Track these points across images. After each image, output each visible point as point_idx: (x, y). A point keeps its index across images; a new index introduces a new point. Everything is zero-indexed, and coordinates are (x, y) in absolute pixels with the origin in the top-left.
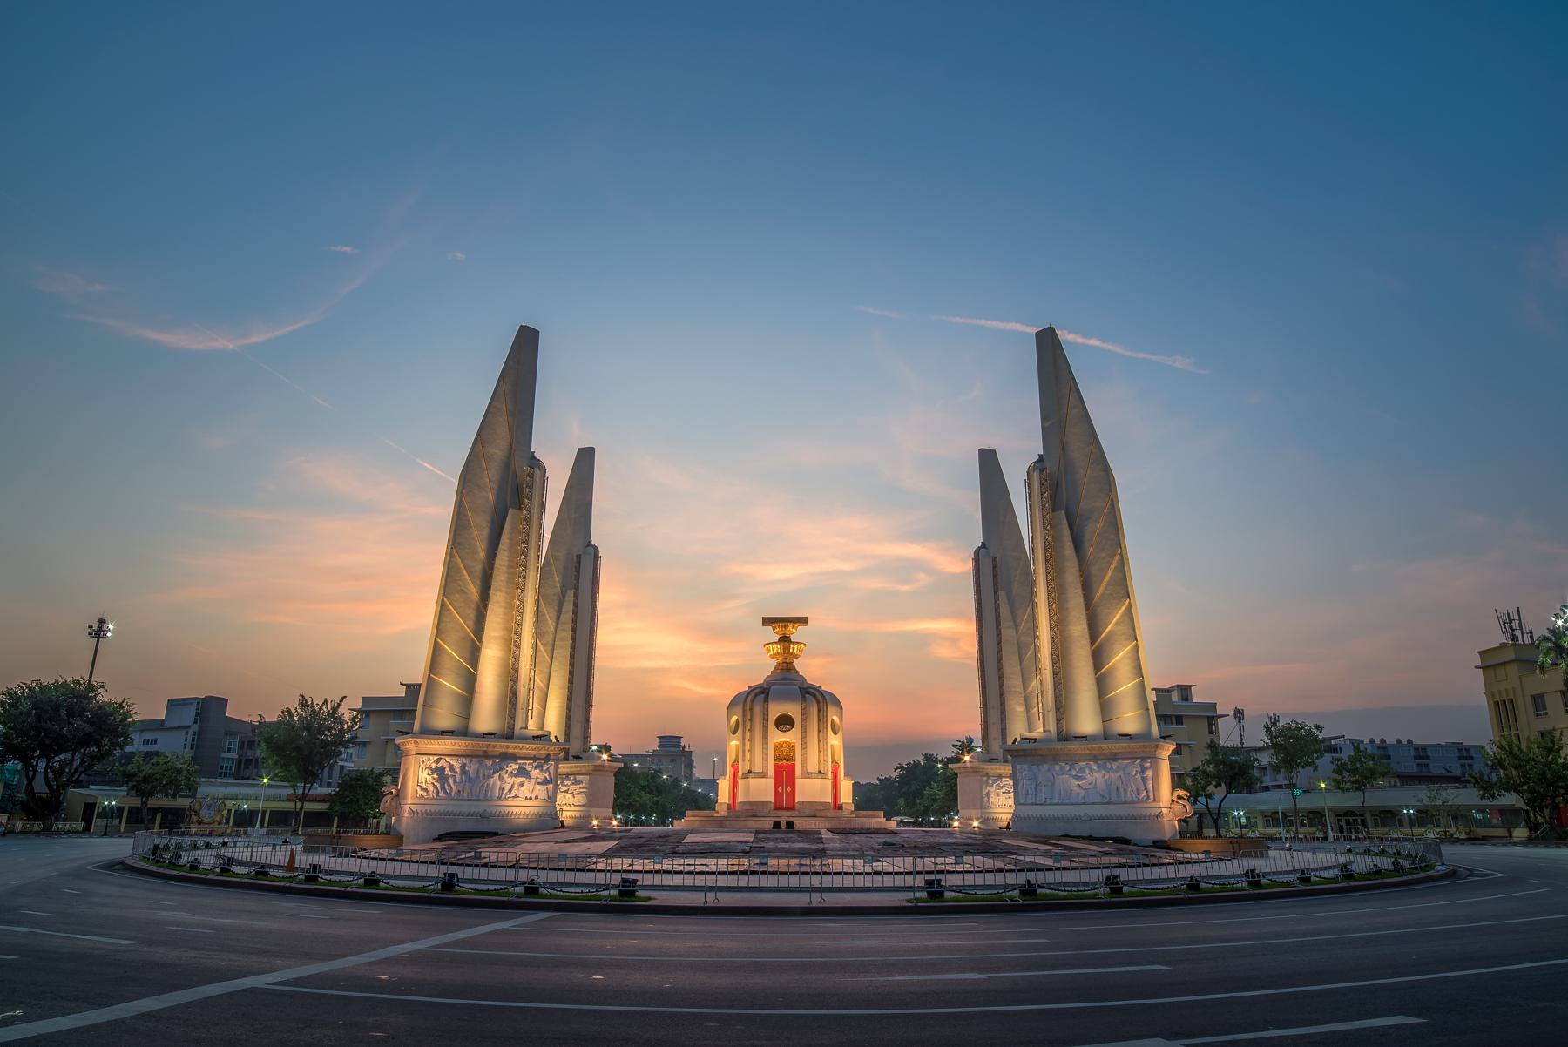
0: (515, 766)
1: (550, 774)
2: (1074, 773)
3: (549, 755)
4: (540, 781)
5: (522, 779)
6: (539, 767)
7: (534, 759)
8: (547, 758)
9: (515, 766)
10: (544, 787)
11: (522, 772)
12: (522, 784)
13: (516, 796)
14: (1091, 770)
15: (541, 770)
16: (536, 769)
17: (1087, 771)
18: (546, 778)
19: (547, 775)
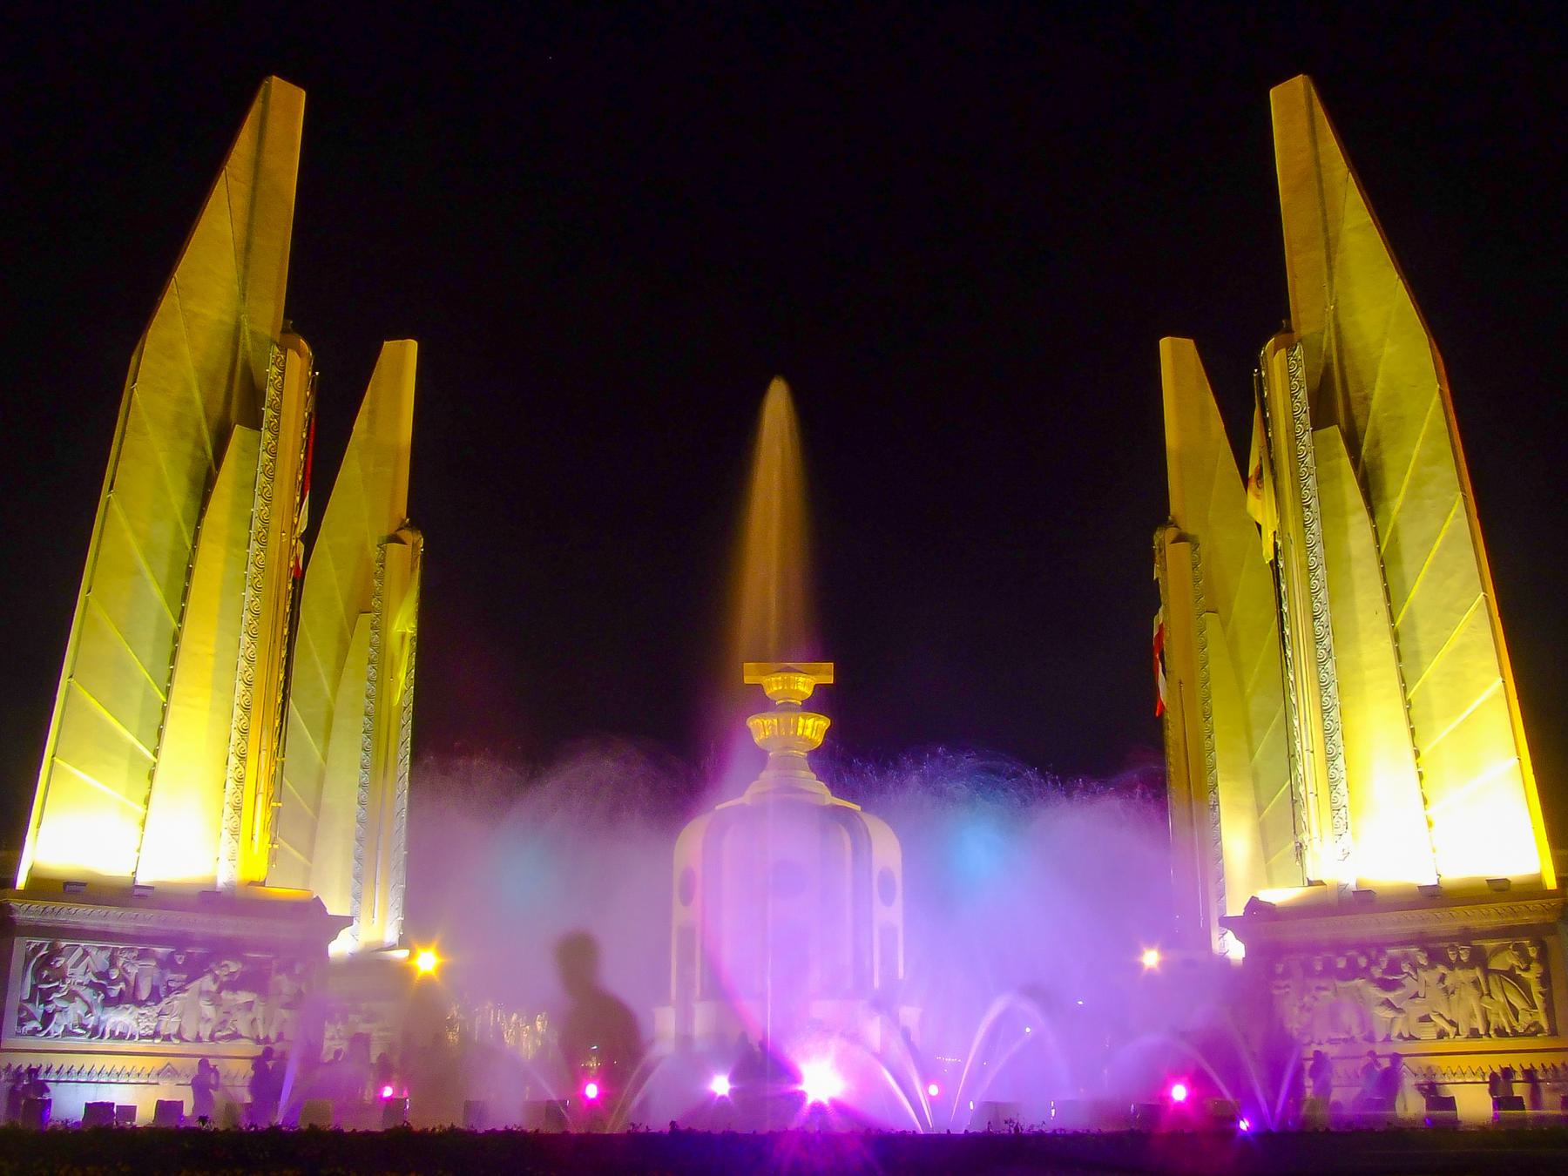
2: (1377, 972)
9: (234, 967)
14: (1415, 967)
17: (1406, 968)
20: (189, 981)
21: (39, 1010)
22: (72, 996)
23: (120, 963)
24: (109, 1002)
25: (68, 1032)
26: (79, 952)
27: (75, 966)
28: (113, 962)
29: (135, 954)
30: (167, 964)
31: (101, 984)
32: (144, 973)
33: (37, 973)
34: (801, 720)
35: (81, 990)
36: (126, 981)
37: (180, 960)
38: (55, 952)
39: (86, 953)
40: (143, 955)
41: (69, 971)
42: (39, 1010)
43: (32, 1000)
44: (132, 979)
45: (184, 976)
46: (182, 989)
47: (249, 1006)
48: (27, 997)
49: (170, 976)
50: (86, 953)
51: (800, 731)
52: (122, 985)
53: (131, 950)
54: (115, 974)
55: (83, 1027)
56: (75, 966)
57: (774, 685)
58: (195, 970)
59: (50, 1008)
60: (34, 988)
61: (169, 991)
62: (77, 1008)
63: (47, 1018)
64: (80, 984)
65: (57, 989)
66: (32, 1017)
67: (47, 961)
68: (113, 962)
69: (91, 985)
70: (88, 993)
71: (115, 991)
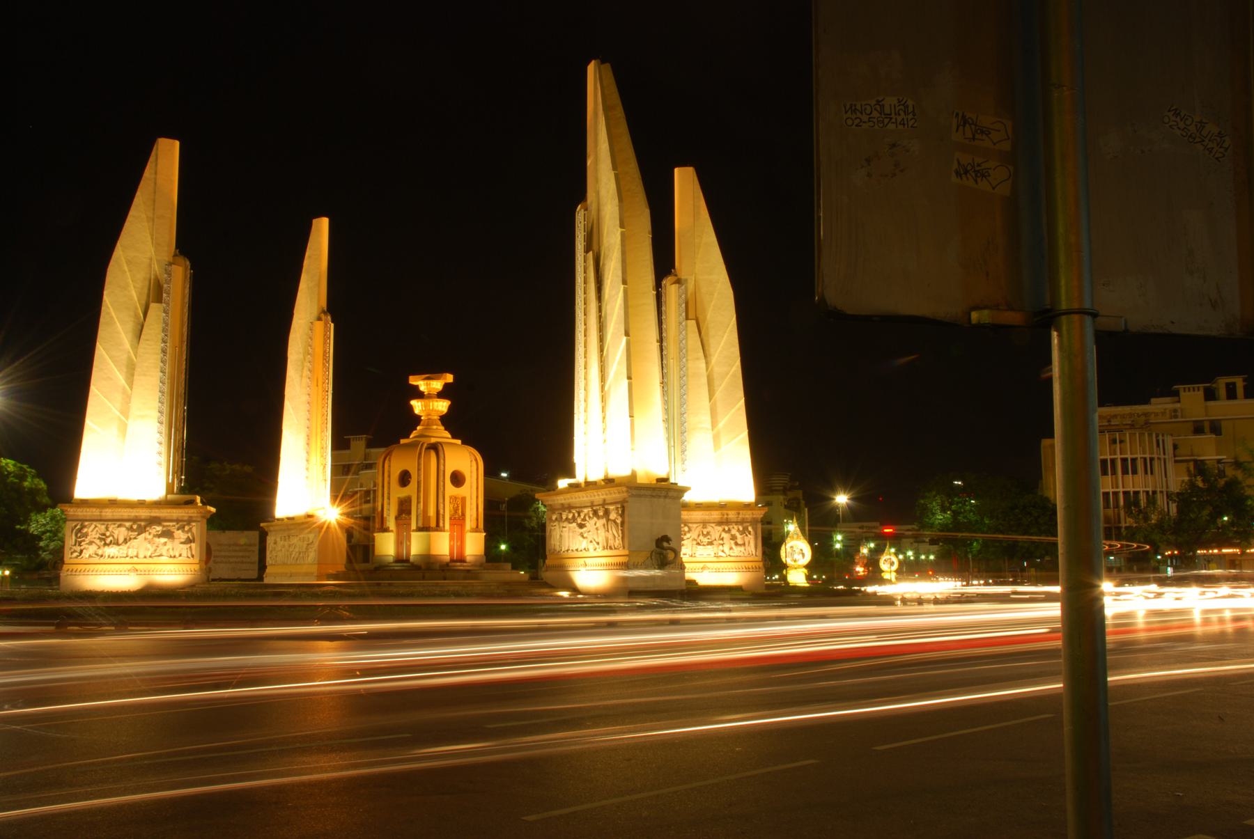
3: (191, 517)
4: (183, 540)
5: (165, 540)
7: (178, 521)
9: (159, 528)
10: (189, 546)
11: (168, 534)
15: (183, 531)
16: (178, 529)
18: (188, 537)
19: (189, 535)
20: (138, 535)
22: (91, 543)
23: (110, 529)
24: (105, 544)
26: (93, 526)
27: (92, 531)
28: (107, 529)
29: (116, 525)
30: (131, 529)
31: (103, 538)
32: (121, 533)
34: (431, 404)
35: (95, 540)
36: (113, 536)
37: (135, 527)
38: (83, 527)
39: (96, 526)
40: (119, 526)
41: (90, 533)
42: (78, 549)
43: (75, 545)
44: (116, 537)
45: (136, 533)
46: (135, 538)
47: (165, 544)
48: (73, 544)
49: (130, 533)
50: (96, 526)
51: (431, 408)
52: (111, 538)
53: (114, 524)
54: (108, 534)
55: (97, 555)
56: (92, 531)
57: (422, 385)
58: (141, 530)
59: (82, 548)
60: (76, 541)
61: (130, 539)
62: (92, 549)
64: (95, 538)
65: (84, 541)
67: (80, 530)
68: (107, 529)
69: (99, 538)
70: (98, 541)
71: (108, 541)
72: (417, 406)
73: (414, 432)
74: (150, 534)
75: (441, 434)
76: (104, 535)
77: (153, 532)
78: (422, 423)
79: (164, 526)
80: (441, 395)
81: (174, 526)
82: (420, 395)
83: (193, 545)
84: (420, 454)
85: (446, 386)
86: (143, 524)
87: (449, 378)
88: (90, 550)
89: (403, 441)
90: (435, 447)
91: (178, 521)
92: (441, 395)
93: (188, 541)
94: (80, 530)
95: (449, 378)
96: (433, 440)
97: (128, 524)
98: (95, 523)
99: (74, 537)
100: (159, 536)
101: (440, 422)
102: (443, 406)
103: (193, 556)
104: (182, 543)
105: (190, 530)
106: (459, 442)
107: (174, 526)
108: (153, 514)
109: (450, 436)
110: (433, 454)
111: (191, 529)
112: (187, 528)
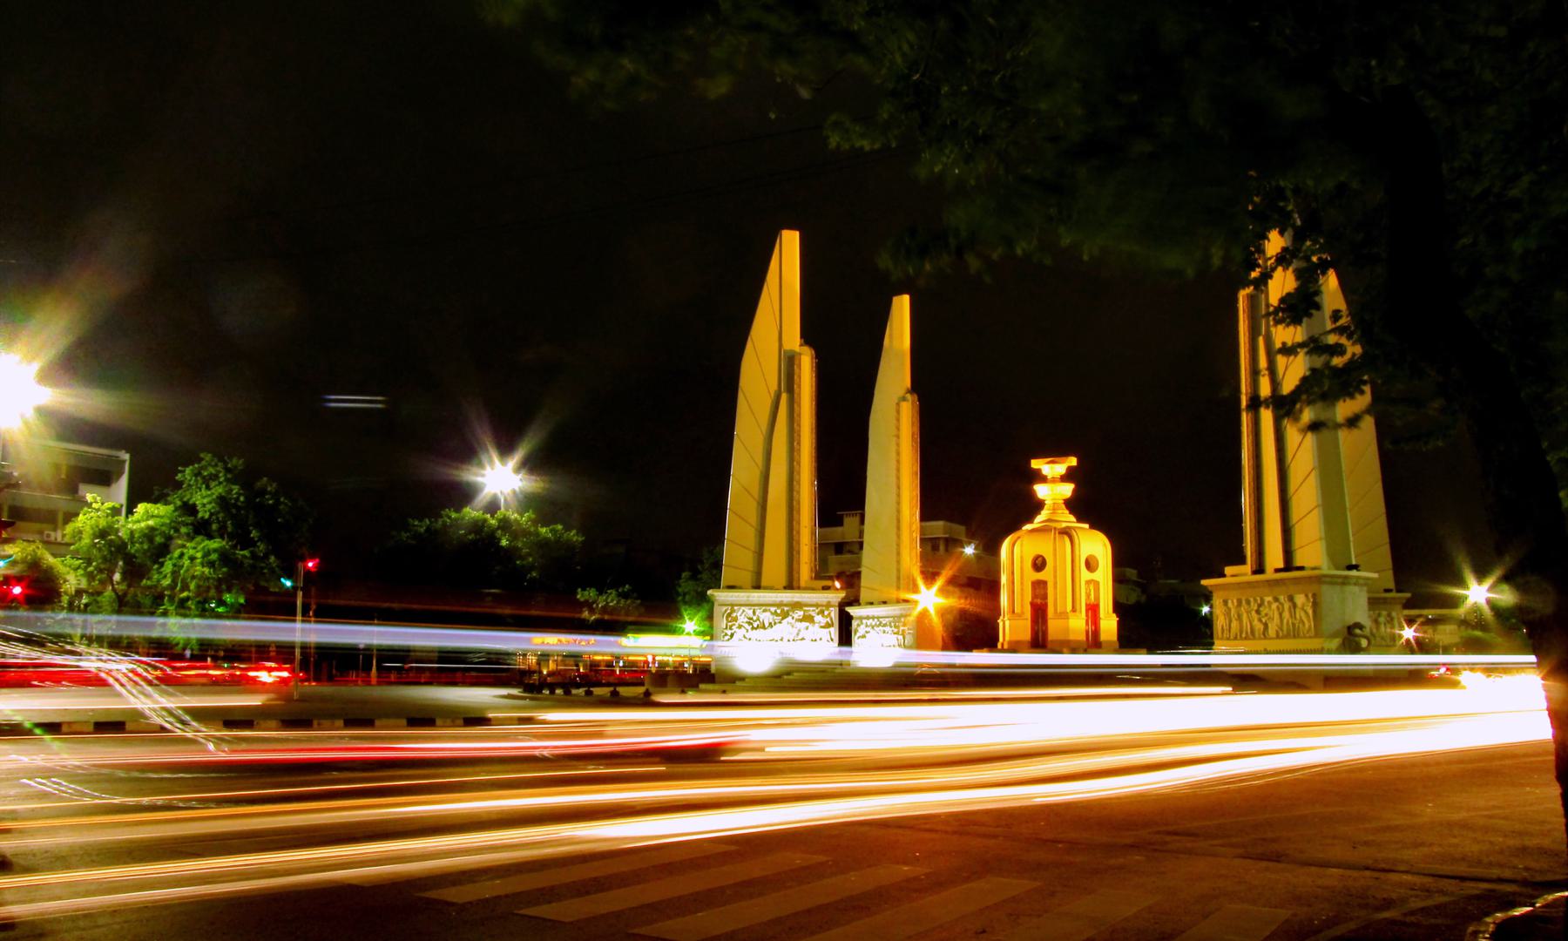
0: (801, 613)
1: (831, 619)
4: (823, 625)
5: (808, 624)
6: (822, 612)
8: (829, 605)
9: (801, 613)
10: (828, 630)
11: (808, 619)
12: (807, 628)
13: (803, 639)
16: (818, 614)
19: (828, 619)
20: (783, 619)
21: (729, 632)
22: (740, 627)
23: (757, 613)
24: (753, 628)
25: (740, 640)
28: (754, 613)
30: (775, 613)
32: (766, 617)
33: (727, 618)
37: (779, 611)
40: (764, 611)
42: (729, 632)
43: (726, 628)
46: (780, 623)
50: (744, 611)
54: (755, 618)
58: (785, 615)
59: (733, 631)
61: (775, 624)
62: (739, 633)
63: (732, 635)
66: (726, 635)
67: (729, 615)
70: (746, 625)
71: (755, 625)
72: (1041, 490)
73: (1039, 517)
74: (793, 618)
75: (1068, 519)
76: (751, 619)
77: (796, 616)
78: (1046, 507)
79: (805, 611)
80: (1065, 478)
81: (813, 611)
82: (1044, 479)
83: (832, 629)
84: (1055, 538)
85: (1070, 469)
86: (786, 609)
87: (1073, 461)
88: (739, 633)
89: (1028, 527)
90: (1066, 532)
91: (817, 606)
92: (1065, 478)
93: (828, 626)
94: (729, 615)
95: (1073, 461)
96: (1064, 525)
97: (773, 609)
98: (743, 608)
99: (725, 622)
100: (801, 621)
101: (1064, 506)
102: (1067, 489)
103: (832, 640)
104: (822, 627)
105: (829, 614)
106: (1087, 526)
107: (813, 611)
108: (796, 600)
109: (1075, 520)
110: (1067, 539)
111: (829, 614)
112: (826, 613)
